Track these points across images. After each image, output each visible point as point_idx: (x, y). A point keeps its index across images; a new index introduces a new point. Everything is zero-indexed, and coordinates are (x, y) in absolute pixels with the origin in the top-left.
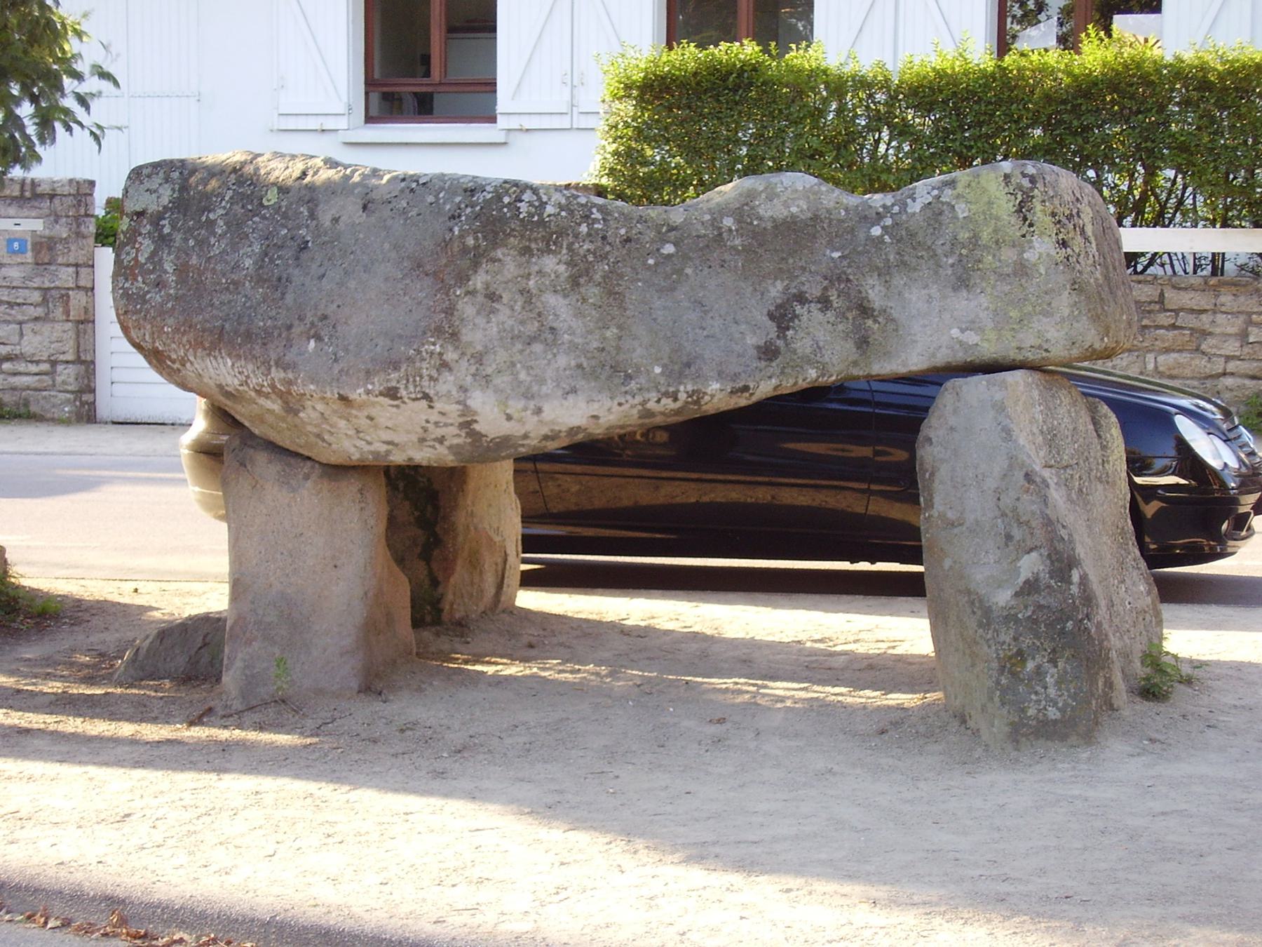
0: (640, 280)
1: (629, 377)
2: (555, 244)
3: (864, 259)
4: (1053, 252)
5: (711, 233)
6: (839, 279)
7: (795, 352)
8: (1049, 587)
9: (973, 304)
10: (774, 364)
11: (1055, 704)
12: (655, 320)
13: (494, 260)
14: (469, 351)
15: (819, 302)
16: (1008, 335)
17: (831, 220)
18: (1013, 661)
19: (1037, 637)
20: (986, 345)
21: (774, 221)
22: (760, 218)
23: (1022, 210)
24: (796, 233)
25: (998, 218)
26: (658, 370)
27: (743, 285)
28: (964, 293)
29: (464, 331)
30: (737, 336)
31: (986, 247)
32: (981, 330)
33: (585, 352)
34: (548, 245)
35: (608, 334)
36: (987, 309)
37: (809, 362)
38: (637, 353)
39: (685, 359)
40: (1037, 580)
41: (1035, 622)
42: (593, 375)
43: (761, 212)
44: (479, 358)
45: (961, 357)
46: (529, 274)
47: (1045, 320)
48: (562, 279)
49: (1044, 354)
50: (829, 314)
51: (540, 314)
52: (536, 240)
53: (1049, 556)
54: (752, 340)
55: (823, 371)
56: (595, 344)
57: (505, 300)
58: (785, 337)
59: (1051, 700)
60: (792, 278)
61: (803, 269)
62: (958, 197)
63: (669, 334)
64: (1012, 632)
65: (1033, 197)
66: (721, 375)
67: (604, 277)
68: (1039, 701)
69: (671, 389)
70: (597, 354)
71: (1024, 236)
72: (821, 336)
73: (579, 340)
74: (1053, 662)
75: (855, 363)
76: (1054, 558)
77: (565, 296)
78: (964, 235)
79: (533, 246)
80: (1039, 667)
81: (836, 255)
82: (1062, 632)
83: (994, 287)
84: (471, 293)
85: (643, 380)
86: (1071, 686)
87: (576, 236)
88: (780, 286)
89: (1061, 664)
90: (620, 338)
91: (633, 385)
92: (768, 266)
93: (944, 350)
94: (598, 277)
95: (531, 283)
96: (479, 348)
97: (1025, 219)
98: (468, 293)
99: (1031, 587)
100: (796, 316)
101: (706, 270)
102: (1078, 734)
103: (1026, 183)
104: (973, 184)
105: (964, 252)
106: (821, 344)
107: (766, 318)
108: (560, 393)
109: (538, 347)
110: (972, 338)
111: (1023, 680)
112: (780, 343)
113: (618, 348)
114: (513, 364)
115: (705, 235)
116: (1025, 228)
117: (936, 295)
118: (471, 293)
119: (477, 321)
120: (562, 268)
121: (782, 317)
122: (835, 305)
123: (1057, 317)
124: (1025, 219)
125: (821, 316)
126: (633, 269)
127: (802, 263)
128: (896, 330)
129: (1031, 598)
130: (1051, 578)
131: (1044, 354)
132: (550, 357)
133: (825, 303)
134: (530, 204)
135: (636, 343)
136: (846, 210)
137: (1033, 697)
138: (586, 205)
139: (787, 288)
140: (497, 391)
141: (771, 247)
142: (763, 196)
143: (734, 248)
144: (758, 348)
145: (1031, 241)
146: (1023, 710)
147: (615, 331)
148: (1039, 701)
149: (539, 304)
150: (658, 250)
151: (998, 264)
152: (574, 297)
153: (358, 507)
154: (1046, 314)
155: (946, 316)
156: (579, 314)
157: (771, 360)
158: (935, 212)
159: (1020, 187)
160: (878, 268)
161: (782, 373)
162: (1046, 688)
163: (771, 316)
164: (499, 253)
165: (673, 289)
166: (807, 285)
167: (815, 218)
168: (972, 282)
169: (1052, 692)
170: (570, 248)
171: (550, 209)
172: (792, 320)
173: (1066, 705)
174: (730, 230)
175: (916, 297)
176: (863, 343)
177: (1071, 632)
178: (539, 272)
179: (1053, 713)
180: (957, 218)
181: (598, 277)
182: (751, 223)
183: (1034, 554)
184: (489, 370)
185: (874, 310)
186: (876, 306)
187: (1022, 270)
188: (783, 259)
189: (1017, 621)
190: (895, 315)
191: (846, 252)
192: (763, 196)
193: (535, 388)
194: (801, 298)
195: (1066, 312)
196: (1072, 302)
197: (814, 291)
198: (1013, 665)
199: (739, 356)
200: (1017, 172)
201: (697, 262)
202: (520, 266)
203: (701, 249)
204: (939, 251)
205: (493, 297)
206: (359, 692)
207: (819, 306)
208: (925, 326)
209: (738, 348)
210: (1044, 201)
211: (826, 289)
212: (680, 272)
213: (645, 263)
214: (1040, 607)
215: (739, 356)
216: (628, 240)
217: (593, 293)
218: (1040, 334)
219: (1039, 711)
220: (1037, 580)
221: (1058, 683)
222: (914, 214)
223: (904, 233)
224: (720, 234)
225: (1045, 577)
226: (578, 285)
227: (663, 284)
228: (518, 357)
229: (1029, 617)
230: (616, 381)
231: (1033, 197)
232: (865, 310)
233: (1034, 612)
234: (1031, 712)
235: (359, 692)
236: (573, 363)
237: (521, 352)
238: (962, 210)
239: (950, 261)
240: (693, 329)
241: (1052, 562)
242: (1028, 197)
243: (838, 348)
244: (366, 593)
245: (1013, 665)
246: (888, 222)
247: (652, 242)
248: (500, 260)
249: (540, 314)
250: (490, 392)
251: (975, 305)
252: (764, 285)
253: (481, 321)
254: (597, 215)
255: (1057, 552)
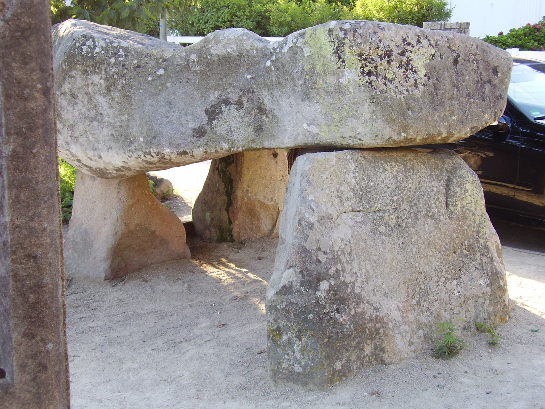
0: (141, 89)
1: (131, 142)
2: (98, 68)
3: (261, 80)
4: (357, 79)
5: (184, 63)
6: (248, 91)
7: (215, 133)
8: (299, 291)
9: (313, 109)
10: (201, 139)
11: (300, 363)
12: (144, 111)
13: (72, 77)
14: (67, 124)
15: (236, 104)
16: (335, 129)
17: (249, 56)
18: (275, 333)
19: (289, 320)
20: (323, 134)
21: (218, 56)
22: (211, 55)
23: (338, 53)
24: (230, 63)
25: (325, 57)
26: (142, 140)
27: (196, 93)
28: (307, 102)
29: (63, 113)
30: (184, 122)
31: (319, 75)
32: (318, 125)
33: (114, 127)
34: (95, 69)
35: (123, 118)
36: (321, 112)
37: (223, 139)
38: (135, 130)
39: (153, 134)
40: (291, 286)
41: (288, 312)
42: (117, 140)
43: (212, 51)
44: (72, 128)
45: (310, 141)
46: (88, 85)
47: (355, 121)
48: (103, 87)
49: (360, 142)
50: (241, 111)
51: (95, 106)
52: (89, 66)
53: (301, 272)
54: (192, 125)
55: (232, 143)
56: (118, 124)
57: (80, 98)
58: (212, 123)
59: (297, 360)
60: (224, 90)
61: (230, 84)
62: (305, 43)
63: (148, 120)
64: (273, 316)
65: (344, 44)
66: (170, 145)
67: (122, 87)
68: (289, 360)
69: (147, 151)
70: (119, 129)
71: (339, 68)
72: (233, 124)
73: (112, 121)
74: (299, 338)
75: (253, 141)
76: (305, 273)
77: (105, 97)
78: (307, 67)
79: (88, 69)
80: (289, 339)
81: (249, 77)
82: (305, 320)
83: (324, 99)
84: (63, 94)
85: (136, 144)
86: (310, 353)
87: (109, 64)
88: (217, 94)
89: (304, 340)
90: (129, 120)
91: (133, 147)
92: (212, 82)
93: (301, 135)
94: (119, 87)
95: (90, 89)
96: (71, 122)
97: (340, 58)
98: (62, 94)
99: (286, 290)
100: (221, 112)
101: (178, 84)
102: (314, 383)
103: (341, 35)
104: (313, 35)
105: (307, 77)
106: (233, 129)
107: (203, 113)
108: (105, 149)
109: (95, 124)
110: (314, 130)
111: (279, 346)
112: (208, 128)
113: (128, 126)
114: (86, 132)
115: (181, 64)
116: (340, 63)
117: (294, 103)
118: (63, 94)
119: (68, 108)
120: (102, 81)
121: (213, 113)
122: (245, 106)
123: (362, 120)
124: (340, 58)
125: (235, 112)
126: (139, 83)
127: (230, 81)
128: (277, 122)
129: (286, 297)
130: (302, 285)
131: (360, 142)
132: (100, 129)
133: (240, 105)
134: (89, 47)
135: (135, 124)
136: (257, 50)
137: (286, 356)
138: (117, 47)
139: (220, 96)
140: (82, 145)
141: (216, 72)
142: (213, 41)
143: (195, 72)
144: (194, 129)
145: (343, 72)
146: (280, 363)
147: (127, 117)
148: (289, 360)
149: (95, 101)
150: (155, 72)
151: (325, 85)
152: (108, 98)
153: (117, 191)
154: (356, 117)
155: (300, 115)
156: (111, 107)
157: (200, 137)
158: (295, 51)
159: (337, 37)
160: (268, 85)
161: (206, 144)
162: (294, 353)
163: (207, 112)
164: (73, 73)
165: (157, 95)
166: (231, 94)
167: (240, 55)
168: (311, 96)
169: (298, 355)
170: (106, 72)
171: (97, 50)
172: (218, 114)
173: (307, 364)
174: (194, 61)
175: (284, 102)
176: (259, 129)
177: (311, 321)
178: (92, 83)
179: (298, 368)
180: (304, 56)
181: (119, 87)
182: (207, 58)
183: (291, 270)
184: (77, 135)
185: (266, 110)
186: (268, 108)
187: (339, 89)
188: (221, 78)
189: (276, 310)
190: (277, 114)
191: (254, 76)
192: (213, 41)
193: (96, 145)
194: (227, 102)
195: (368, 116)
196: (371, 111)
197: (234, 98)
198: (274, 336)
199: (182, 134)
200: (338, 28)
201: (174, 80)
202: (83, 80)
203: (177, 72)
204: (295, 77)
205: (74, 96)
206: (105, 280)
207: (237, 106)
208: (290, 121)
209: (182, 129)
210: (352, 46)
211: (241, 96)
212: (163, 85)
213: (146, 79)
214: (291, 303)
215: (182, 134)
216: (139, 67)
217: (117, 95)
218: (353, 130)
219: (290, 365)
220: (291, 286)
221: (302, 351)
222: (284, 54)
223: (280, 65)
224: (188, 64)
225: (297, 285)
226: (110, 91)
227: (153, 91)
228: (88, 128)
229: (284, 309)
230: (126, 144)
231: (344, 44)
232: (261, 110)
233: (286, 306)
234: (284, 365)
235: (105, 280)
236: (110, 133)
237: (89, 125)
238: (307, 52)
239: (300, 83)
240: (162, 117)
241: (303, 276)
242: (341, 44)
243: (242, 131)
244: (116, 233)
245: (274, 336)
246: (274, 58)
247: (153, 67)
248: (74, 77)
249: (95, 106)
250: (78, 145)
251: (314, 109)
252: (208, 93)
253: (70, 108)
254: (122, 53)
255: (308, 270)
